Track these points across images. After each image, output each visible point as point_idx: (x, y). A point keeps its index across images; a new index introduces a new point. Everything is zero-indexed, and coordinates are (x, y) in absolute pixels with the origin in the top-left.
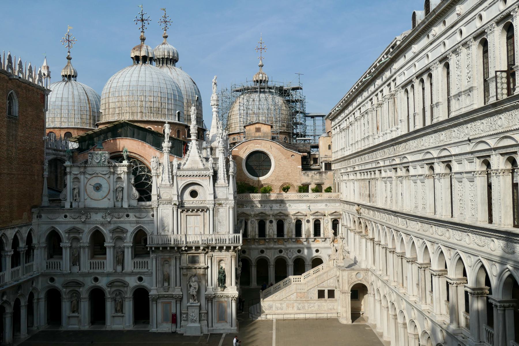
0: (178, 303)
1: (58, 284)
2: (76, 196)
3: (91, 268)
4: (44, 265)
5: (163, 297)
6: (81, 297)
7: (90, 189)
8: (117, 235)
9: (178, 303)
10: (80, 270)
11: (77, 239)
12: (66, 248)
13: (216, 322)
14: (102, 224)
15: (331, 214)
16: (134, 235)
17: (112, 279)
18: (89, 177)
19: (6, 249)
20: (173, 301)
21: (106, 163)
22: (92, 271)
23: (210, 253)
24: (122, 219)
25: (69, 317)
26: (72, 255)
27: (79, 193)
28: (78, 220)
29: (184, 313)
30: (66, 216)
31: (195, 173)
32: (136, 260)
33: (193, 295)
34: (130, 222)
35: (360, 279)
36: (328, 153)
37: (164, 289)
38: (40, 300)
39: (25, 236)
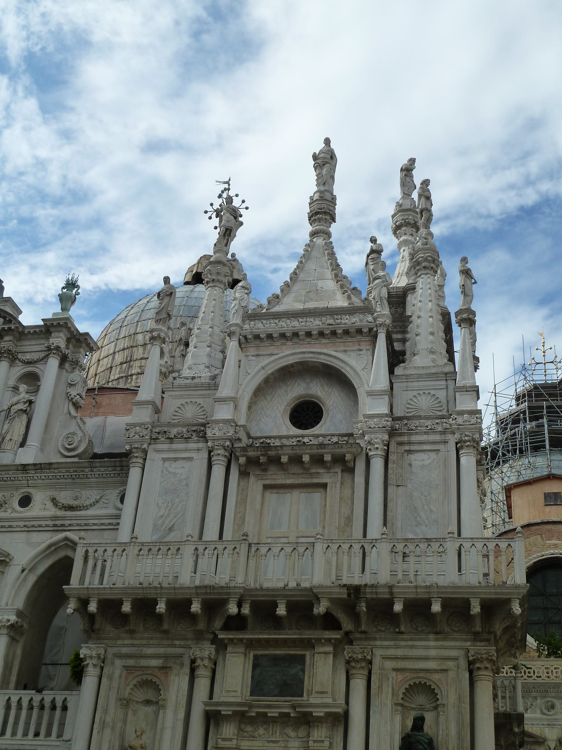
16: (32, 579)
31: (315, 324)
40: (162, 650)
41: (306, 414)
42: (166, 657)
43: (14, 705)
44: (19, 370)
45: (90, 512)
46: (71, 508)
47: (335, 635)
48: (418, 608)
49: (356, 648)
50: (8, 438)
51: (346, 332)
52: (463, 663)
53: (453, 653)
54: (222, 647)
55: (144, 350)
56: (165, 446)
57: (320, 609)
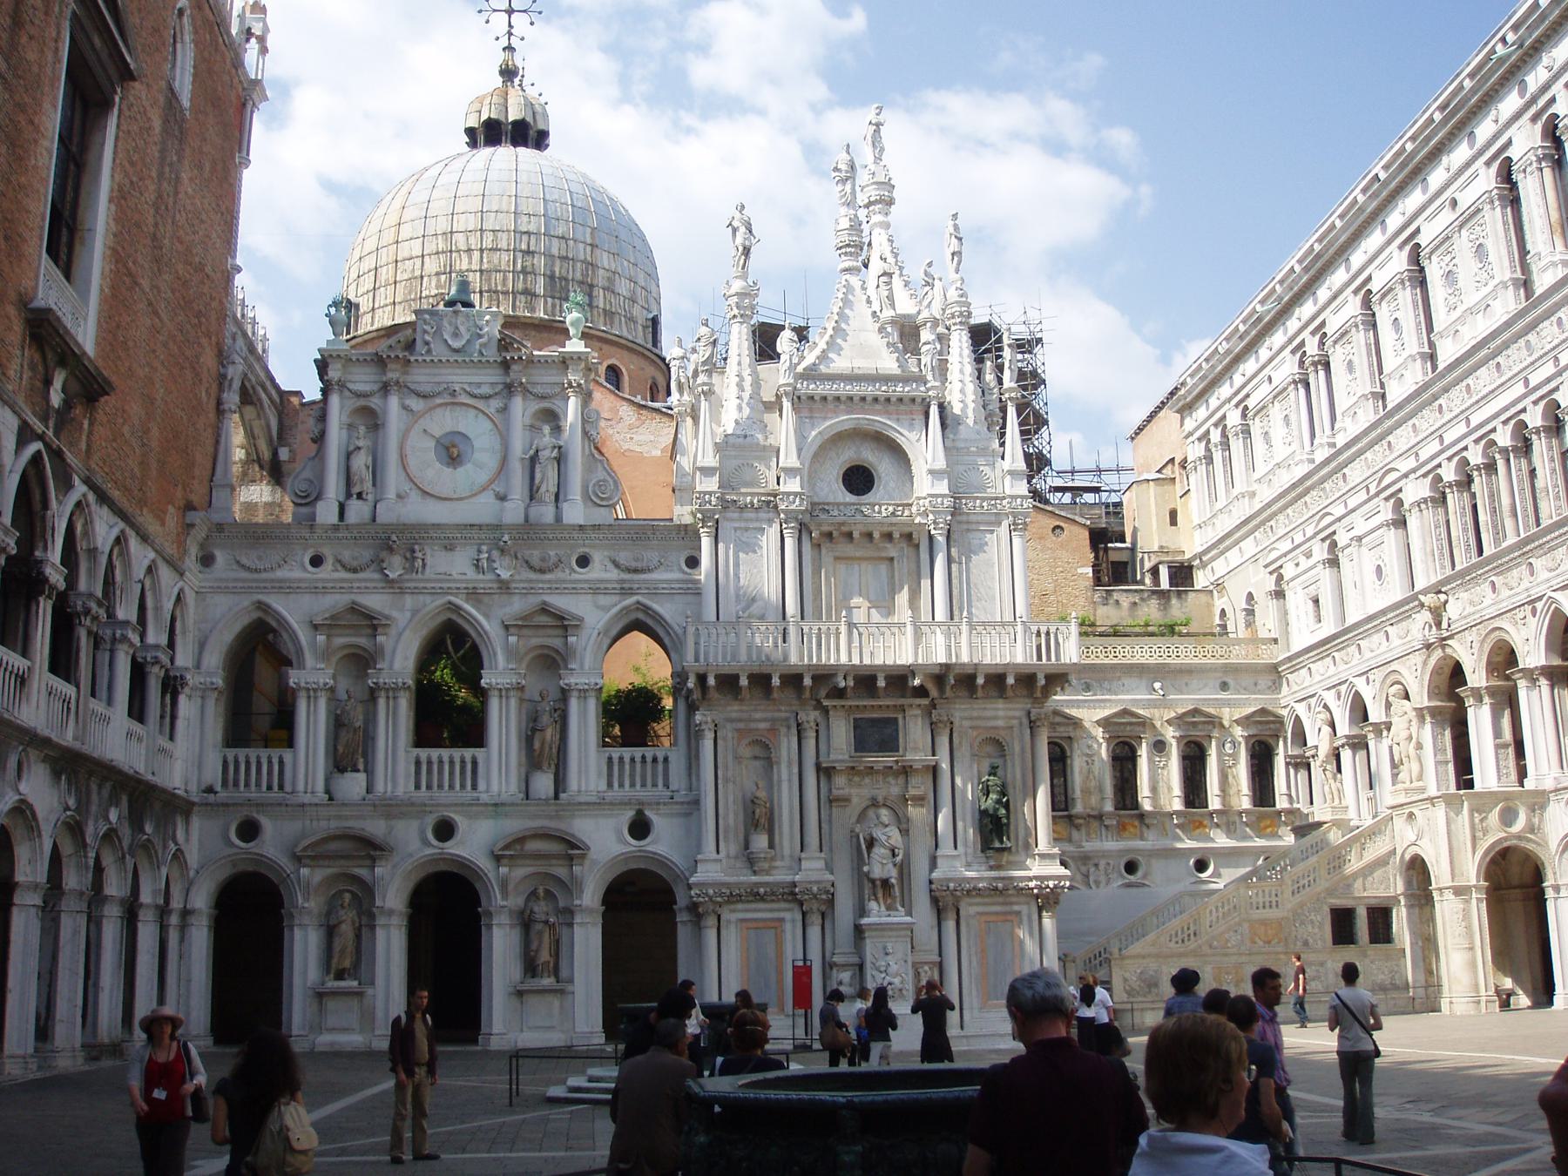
0: (815, 919)
2: (362, 481)
3: (418, 787)
4: (213, 774)
5: (755, 895)
6: (378, 903)
7: (422, 453)
8: (535, 641)
9: (815, 919)
11: (361, 661)
12: (312, 693)
13: (976, 1005)
14: (473, 595)
15: (1244, 722)
17: (513, 825)
18: (416, 404)
19: (121, 614)
21: (492, 354)
25: (320, 996)
26: (338, 723)
27: (376, 470)
28: (369, 574)
29: (844, 966)
30: (317, 561)
31: (869, 390)
33: (886, 883)
34: (596, 589)
37: (751, 861)
38: (193, 920)
39: (168, 605)
40: (769, 715)
42: (773, 720)
43: (616, 761)
44: (535, 406)
45: (655, 576)
46: (636, 571)
47: (925, 702)
48: (997, 680)
49: (943, 712)
50: (543, 489)
51: (900, 400)
52: (1025, 721)
53: (1017, 714)
55: (470, 258)
56: (736, 515)
57: (917, 682)
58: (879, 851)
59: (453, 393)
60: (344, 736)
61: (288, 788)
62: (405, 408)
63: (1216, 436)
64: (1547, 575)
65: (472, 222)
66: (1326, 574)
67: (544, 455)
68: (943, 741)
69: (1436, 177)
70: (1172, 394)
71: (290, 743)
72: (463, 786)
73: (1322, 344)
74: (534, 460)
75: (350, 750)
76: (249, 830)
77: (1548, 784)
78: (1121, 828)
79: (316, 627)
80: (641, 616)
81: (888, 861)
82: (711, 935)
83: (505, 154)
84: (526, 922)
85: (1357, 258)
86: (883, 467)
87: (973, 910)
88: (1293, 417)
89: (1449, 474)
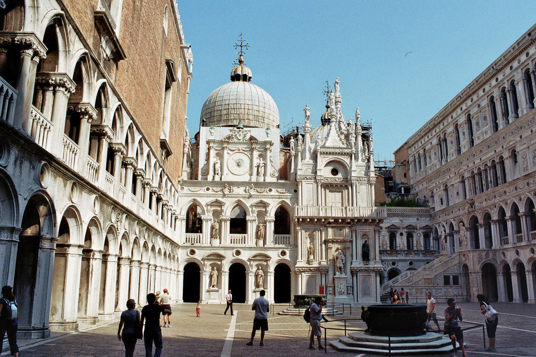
1: (199, 256)
3: (231, 243)
10: (220, 244)
12: (207, 220)
14: (244, 198)
15: (423, 228)
20: (319, 274)
22: (233, 245)
23: (354, 228)
24: (264, 194)
25: (208, 291)
28: (220, 193)
30: (208, 189)
32: (278, 235)
33: (340, 268)
35: (489, 258)
36: (404, 180)
38: (179, 273)
41: (335, 172)
48: (366, 220)
54: (327, 227)
58: (339, 260)
59: (239, 150)
60: (214, 230)
61: (201, 242)
62: (228, 153)
63: (417, 156)
64: (499, 198)
65: (235, 102)
66: (444, 194)
67: (261, 165)
68: (354, 235)
69: (475, 97)
70: (406, 144)
71: (201, 232)
72: (242, 243)
73: (445, 136)
74: (258, 167)
75: (215, 233)
76: (193, 252)
77: (498, 248)
78: (391, 254)
79: (208, 205)
80: (283, 204)
81: (341, 262)
82: (300, 279)
83: (241, 83)
84: (256, 276)
85: (455, 115)
86: (340, 168)
87: (360, 274)
88: (437, 153)
89: (476, 172)
